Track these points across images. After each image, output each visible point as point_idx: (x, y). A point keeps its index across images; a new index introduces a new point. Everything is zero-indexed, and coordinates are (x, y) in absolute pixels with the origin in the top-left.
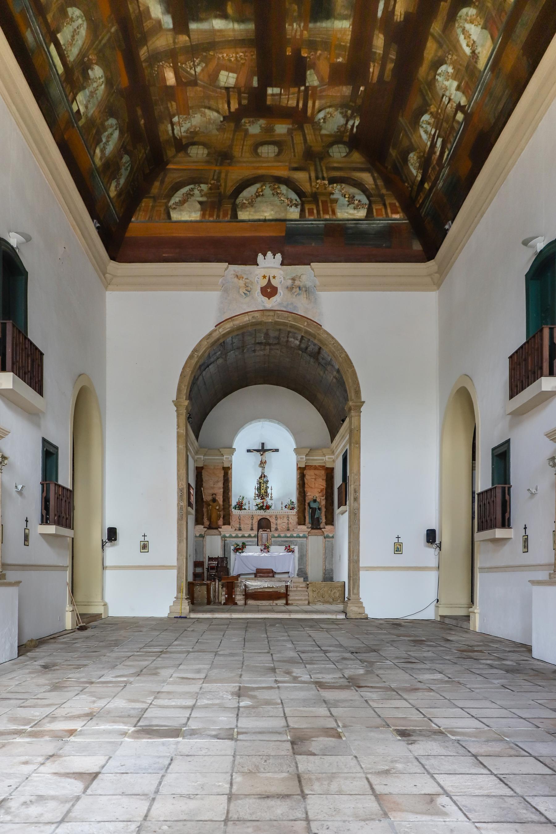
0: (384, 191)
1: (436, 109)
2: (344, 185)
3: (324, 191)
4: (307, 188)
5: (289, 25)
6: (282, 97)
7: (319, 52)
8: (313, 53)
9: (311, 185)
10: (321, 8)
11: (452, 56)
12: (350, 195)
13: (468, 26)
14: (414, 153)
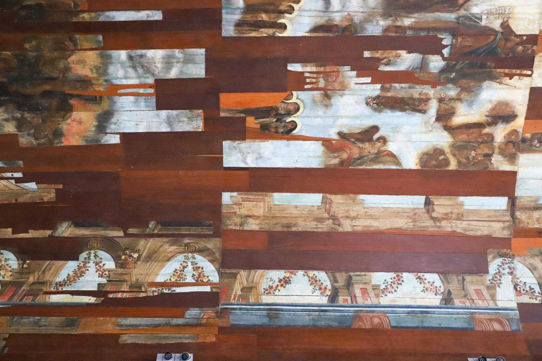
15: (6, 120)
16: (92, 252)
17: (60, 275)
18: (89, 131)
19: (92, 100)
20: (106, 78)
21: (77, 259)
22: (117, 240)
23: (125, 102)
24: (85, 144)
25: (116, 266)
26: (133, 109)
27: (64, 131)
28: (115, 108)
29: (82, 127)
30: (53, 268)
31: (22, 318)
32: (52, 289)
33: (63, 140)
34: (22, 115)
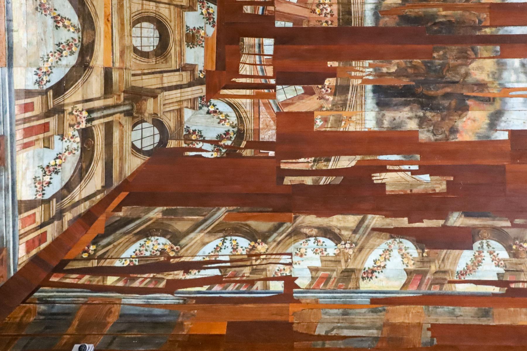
0: (68, 216)
1: (263, 251)
2: (78, 153)
3: (66, 124)
4: (73, 96)
5: (369, 64)
6: (257, 57)
7: (331, 98)
8: (329, 91)
9: (78, 102)
10: (385, 96)
11: (350, 248)
12: (60, 165)
13: (395, 253)
14: (168, 242)
15: (410, 118)
16: (484, 241)
17: (459, 264)
18: (481, 128)
19: (487, 101)
20: (501, 82)
21: (471, 248)
22: (506, 230)
23: (515, 103)
24: (477, 140)
25: (510, 256)
26: (521, 109)
27: (460, 128)
28: (506, 108)
29: (476, 124)
30: (451, 257)
31: (437, 308)
32: (455, 279)
33: (458, 135)
34: (424, 114)
